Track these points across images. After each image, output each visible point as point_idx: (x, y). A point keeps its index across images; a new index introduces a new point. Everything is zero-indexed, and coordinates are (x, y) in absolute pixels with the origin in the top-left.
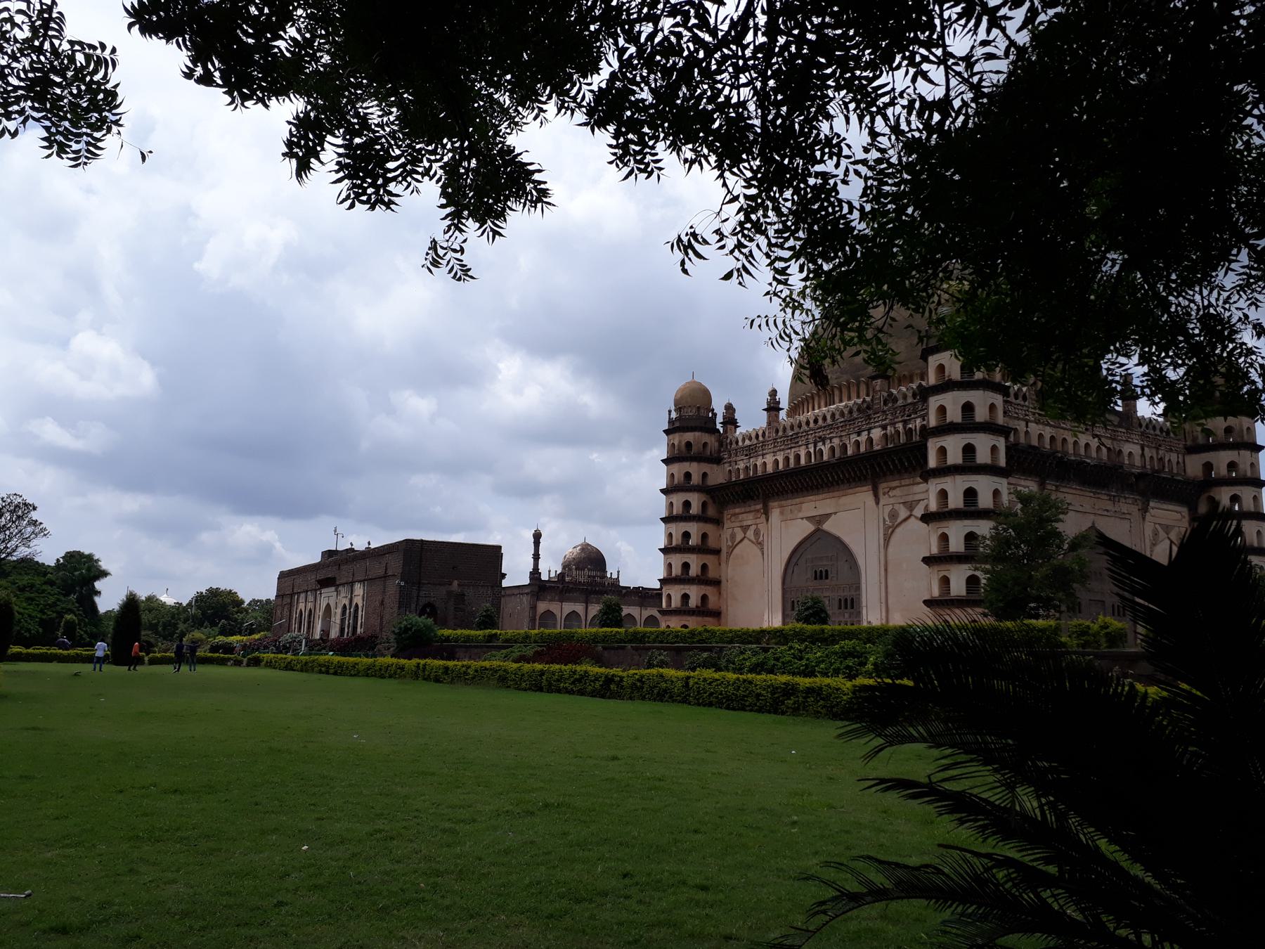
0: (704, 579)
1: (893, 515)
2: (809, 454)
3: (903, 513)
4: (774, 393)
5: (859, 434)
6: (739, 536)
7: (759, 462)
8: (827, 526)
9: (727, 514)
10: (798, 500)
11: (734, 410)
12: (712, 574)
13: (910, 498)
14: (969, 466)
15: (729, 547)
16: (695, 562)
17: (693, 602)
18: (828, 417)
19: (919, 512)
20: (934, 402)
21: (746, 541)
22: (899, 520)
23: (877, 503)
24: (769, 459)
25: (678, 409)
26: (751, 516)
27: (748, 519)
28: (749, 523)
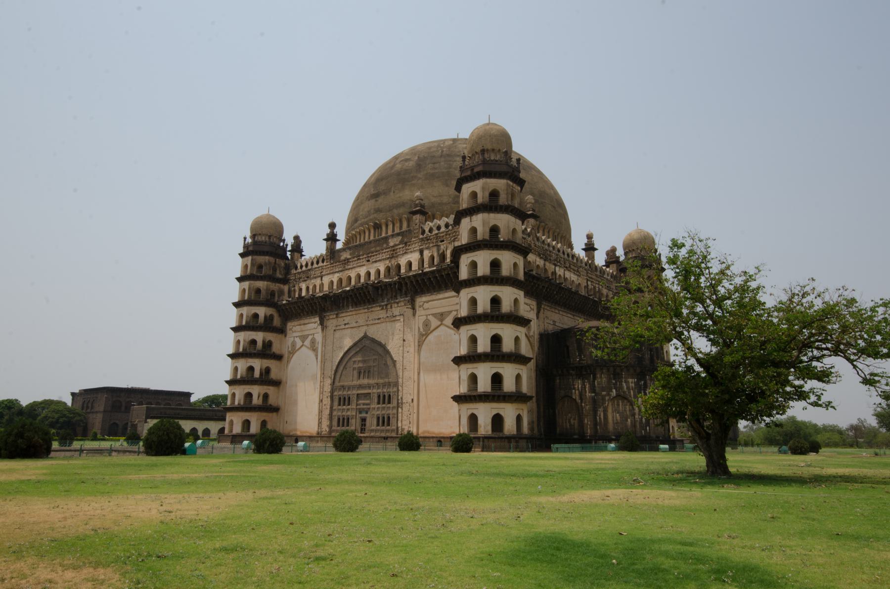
0: (266, 379)
1: (427, 324)
3: (434, 322)
4: (332, 226)
6: (299, 342)
9: (290, 325)
11: (300, 242)
12: (273, 375)
14: (495, 277)
15: (290, 353)
16: (258, 364)
17: (256, 401)
19: (449, 321)
20: (466, 223)
21: (304, 348)
22: (432, 328)
24: (326, 280)
25: (253, 236)
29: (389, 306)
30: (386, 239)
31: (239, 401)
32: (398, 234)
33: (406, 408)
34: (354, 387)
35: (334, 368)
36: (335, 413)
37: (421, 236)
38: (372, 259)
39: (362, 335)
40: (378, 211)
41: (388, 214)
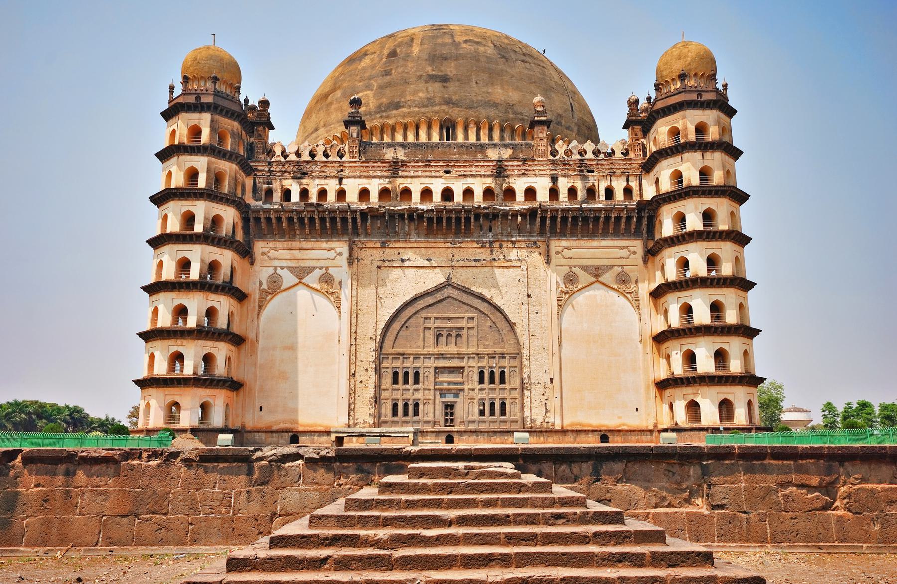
3: (584, 277)
6: (289, 279)
7: (332, 186)
22: (580, 286)
29: (496, 245)
30: (482, 148)
31: (196, 367)
32: (506, 146)
33: (537, 391)
34: (427, 356)
35: (382, 325)
36: (385, 394)
37: (551, 158)
38: (455, 172)
39: (443, 280)
40: (448, 102)
41: (471, 112)
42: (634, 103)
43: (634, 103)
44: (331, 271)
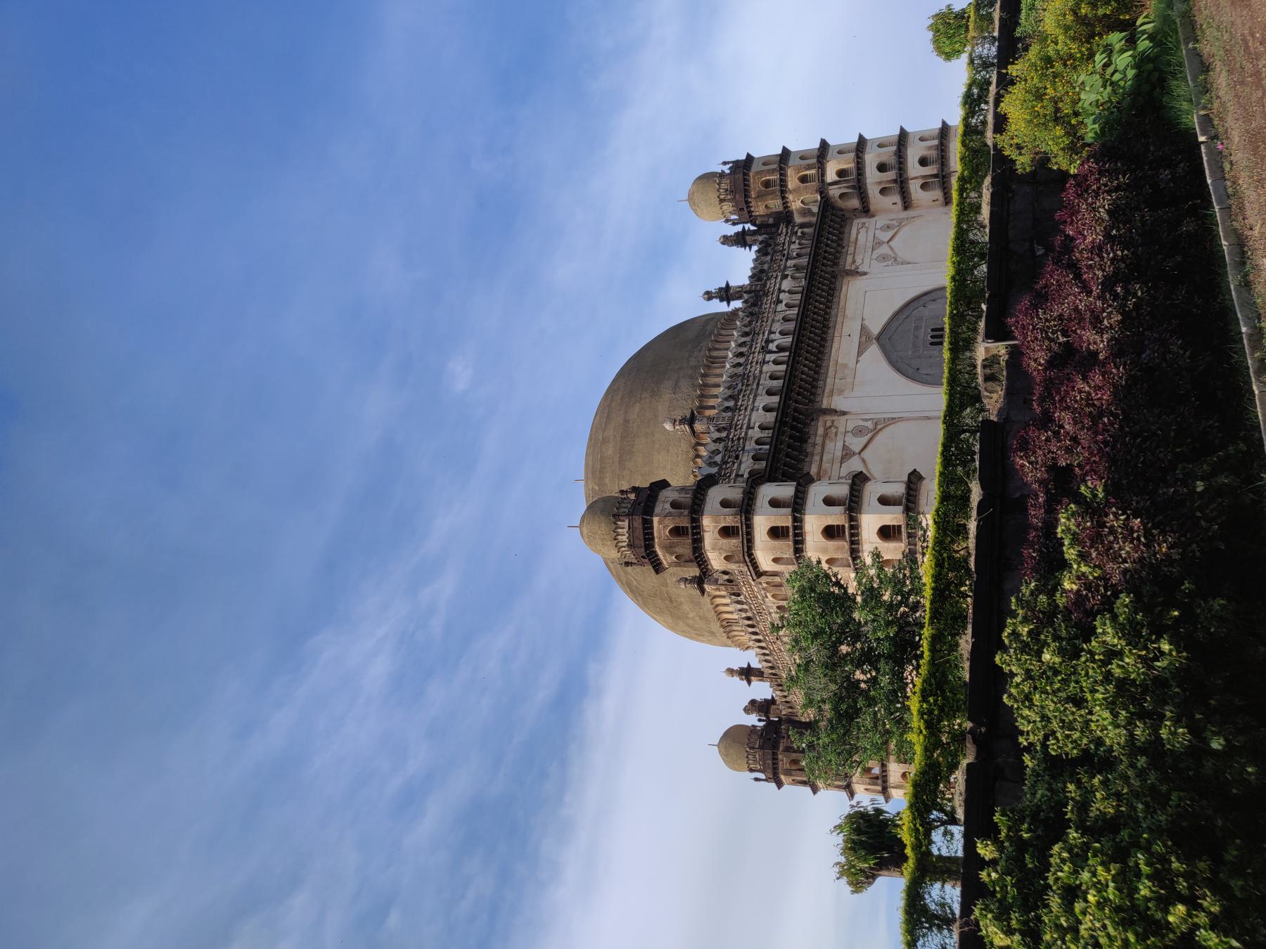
1: (884, 258)
2: (776, 362)
3: (884, 250)
5: (779, 301)
7: (756, 433)
8: (875, 329)
10: (831, 369)
13: (870, 244)
18: (743, 339)
19: (885, 236)
22: (890, 253)
23: (865, 274)
26: (830, 445)
27: (834, 448)
28: (840, 445)
42: (726, 240)
43: (726, 240)
44: (849, 429)
